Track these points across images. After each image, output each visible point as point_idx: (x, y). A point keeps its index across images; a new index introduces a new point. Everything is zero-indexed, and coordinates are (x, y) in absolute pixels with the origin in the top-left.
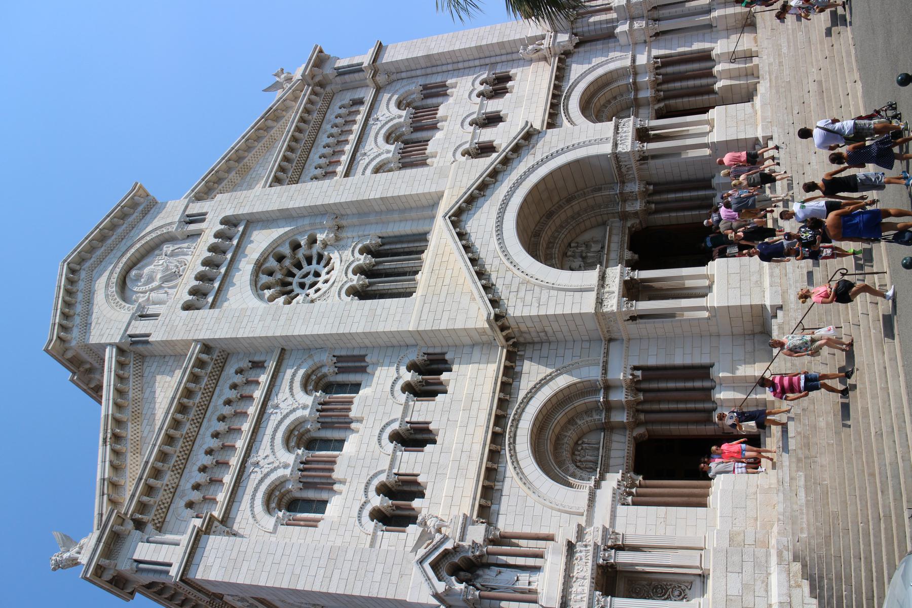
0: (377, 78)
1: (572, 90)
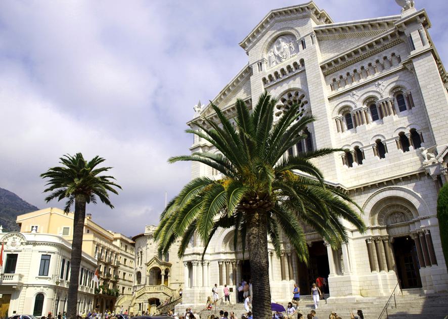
0: (406, 65)
1: (397, 190)
